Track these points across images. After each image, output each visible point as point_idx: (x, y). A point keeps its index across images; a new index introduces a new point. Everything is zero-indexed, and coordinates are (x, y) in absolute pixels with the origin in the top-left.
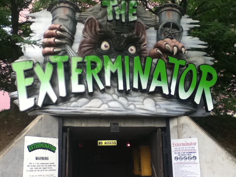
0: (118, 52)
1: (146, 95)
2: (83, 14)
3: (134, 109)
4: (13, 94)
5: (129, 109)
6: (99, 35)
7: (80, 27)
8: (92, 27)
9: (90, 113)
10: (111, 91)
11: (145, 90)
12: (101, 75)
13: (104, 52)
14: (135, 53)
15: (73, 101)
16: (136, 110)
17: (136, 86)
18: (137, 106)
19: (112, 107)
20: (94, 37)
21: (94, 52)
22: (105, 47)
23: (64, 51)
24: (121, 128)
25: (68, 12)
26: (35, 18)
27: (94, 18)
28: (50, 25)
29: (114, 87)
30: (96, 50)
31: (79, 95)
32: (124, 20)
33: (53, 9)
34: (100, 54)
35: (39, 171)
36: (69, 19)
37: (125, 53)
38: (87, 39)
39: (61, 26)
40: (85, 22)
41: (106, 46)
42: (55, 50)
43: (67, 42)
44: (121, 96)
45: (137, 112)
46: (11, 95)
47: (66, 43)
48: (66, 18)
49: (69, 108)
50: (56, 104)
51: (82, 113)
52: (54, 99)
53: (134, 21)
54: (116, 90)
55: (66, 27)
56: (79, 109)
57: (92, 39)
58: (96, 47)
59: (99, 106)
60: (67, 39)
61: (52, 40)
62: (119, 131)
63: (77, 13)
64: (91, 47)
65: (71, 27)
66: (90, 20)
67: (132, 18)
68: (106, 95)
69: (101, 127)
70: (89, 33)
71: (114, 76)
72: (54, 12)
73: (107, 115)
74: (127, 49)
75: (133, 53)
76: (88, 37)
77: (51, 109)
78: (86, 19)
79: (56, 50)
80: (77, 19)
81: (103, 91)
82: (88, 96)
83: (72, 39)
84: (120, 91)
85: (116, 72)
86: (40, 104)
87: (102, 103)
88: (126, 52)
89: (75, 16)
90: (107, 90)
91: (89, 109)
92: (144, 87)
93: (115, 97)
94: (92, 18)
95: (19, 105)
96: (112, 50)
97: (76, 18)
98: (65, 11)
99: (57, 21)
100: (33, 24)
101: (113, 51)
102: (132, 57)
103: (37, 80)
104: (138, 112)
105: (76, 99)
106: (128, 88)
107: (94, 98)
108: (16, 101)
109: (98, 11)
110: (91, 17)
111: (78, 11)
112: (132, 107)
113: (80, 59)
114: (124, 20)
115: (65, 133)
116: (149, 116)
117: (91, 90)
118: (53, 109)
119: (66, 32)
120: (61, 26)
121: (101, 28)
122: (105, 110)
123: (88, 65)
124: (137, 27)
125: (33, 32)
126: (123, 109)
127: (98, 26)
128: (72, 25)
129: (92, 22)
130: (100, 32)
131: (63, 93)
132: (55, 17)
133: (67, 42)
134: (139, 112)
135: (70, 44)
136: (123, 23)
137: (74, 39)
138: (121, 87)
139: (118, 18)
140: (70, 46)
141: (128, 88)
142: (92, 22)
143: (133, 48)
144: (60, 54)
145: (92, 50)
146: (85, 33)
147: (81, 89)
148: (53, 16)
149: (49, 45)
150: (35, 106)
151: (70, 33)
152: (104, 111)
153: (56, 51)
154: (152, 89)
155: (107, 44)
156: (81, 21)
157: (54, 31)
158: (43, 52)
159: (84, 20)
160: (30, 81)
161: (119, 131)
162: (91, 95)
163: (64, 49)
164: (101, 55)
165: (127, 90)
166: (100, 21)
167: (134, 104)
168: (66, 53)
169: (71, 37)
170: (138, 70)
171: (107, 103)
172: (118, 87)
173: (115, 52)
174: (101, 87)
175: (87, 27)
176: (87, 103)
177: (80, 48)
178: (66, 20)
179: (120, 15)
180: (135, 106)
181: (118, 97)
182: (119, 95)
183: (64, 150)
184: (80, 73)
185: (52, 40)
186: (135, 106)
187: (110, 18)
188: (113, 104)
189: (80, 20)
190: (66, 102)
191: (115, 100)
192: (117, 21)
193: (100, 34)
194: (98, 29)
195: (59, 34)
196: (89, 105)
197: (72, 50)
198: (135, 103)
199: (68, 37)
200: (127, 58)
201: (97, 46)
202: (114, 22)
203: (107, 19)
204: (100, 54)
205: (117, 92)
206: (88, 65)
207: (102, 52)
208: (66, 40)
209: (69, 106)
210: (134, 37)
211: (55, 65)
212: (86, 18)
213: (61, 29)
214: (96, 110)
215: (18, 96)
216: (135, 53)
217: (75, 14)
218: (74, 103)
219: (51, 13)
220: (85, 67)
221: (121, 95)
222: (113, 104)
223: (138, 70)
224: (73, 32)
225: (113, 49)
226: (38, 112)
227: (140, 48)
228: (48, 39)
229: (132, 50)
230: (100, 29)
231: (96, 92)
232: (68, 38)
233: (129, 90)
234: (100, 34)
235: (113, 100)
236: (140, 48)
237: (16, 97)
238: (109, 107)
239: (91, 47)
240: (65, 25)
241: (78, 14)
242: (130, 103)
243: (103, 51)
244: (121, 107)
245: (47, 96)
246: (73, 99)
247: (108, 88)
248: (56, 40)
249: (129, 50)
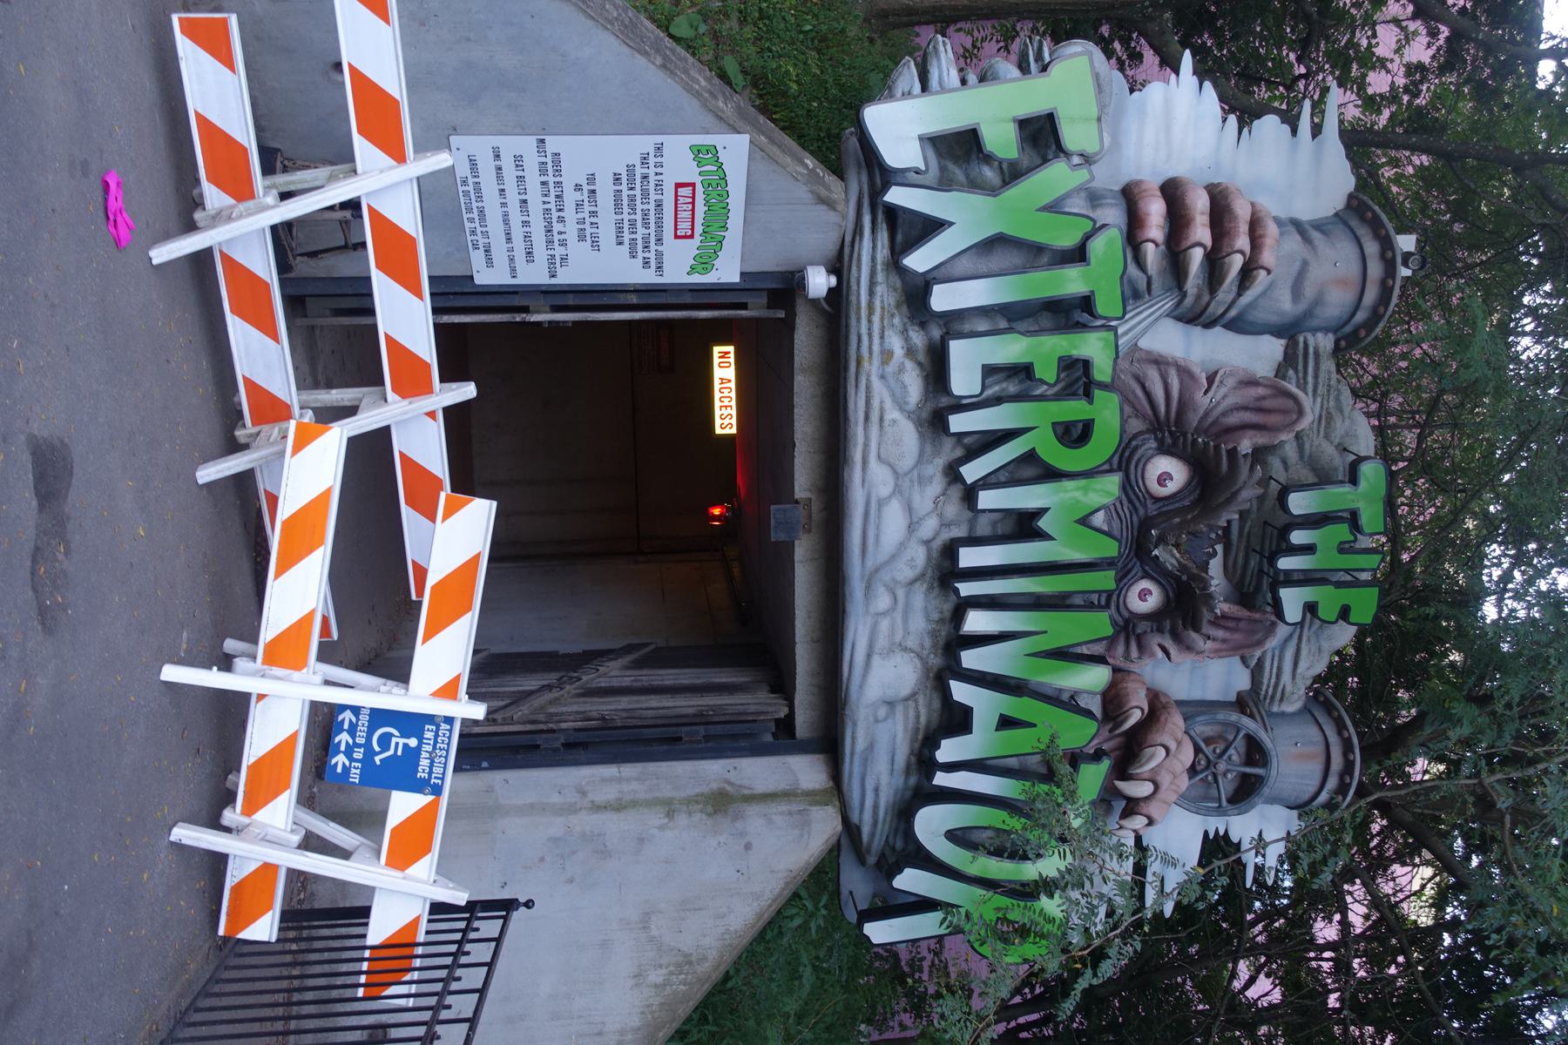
0: (1136, 533)
1: (936, 661)
2: (1328, 365)
3: (872, 610)
4: (943, 55)
5: (868, 588)
6: (1217, 447)
7: (1263, 354)
8: (1260, 410)
9: (847, 596)
10: (953, 508)
11: (958, 661)
12: (1033, 470)
13: (1136, 467)
14: (1130, 612)
15: (907, 339)
16: (869, 621)
17: (977, 622)
18: (884, 624)
19: (879, 517)
20: (1210, 420)
21: (1136, 425)
22: (1165, 473)
23: (1145, 286)
24: (789, 548)
25: (1337, 302)
26: (1314, 136)
27: (1305, 423)
28: (1273, 207)
29: (972, 523)
30: (1148, 431)
31: (936, 369)
32: (1285, 563)
33: (1354, 223)
34: (1127, 454)
35: (593, 214)
36: (1302, 307)
37: (1130, 566)
38: (1204, 390)
39: (1269, 272)
40: (1284, 378)
41: (1163, 479)
42: (1150, 247)
43: (1189, 301)
44: (929, 550)
45: (856, 624)
46: (941, 43)
47: (1184, 295)
48: (1309, 292)
49: (876, 319)
50: (895, 264)
51: (853, 383)
52: (919, 261)
53: (1279, 613)
54: (960, 532)
55: (1263, 294)
56: (872, 368)
57: (1202, 412)
58: (1163, 435)
59: (882, 455)
60: (1206, 298)
61: (1201, 232)
62: (773, 540)
63: (1331, 337)
64: (1162, 409)
65: (1261, 316)
66: (1290, 404)
67: (1292, 600)
68: (937, 485)
69: (794, 457)
70: (1230, 401)
71: (1024, 526)
72: (1339, 231)
73: (845, 535)
74: (1146, 576)
75: (1128, 600)
76: (1210, 394)
77: (874, 241)
78: (1298, 387)
79: (1151, 253)
80: (1301, 339)
81: (952, 473)
82: (930, 406)
83: (1203, 317)
84: (950, 551)
85: (1041, 535)
86: (896, 196)
87: (899, 471)
88: (1133, 573)
89: (1315, 330)
90: (956, 492)
91: (875, 417)
92: (971, 659)
93: (929, 527)
94: (1301, 412)
95: (891, 97)
96: (1145, 506)
97: (1309, 336)
98: (1342, 282)
99: (1293, 243)
100: (1286, 128)
101: (1141, 512)
102: (1108, 600)
103: (1012, 174)
104: (860, 627)
105: (921, 357)
106: (966, 589)
107: (921, 435)
108: (911, 73)
109: (1337, 436)
110: (1308, 409)
111: (1343, 343)
112: (883, 601)
113: (1102, 369)
114: (1285, 563)
115: (764, 301)
116: (842, 676)
117: (959, 423)
118: (872, 249)
119: (1239, 295)
120: (1269, 272)
121: (1250, 459)
122: (866, 485)
123: (1074, 410)
124: (1250, 620)
125: (1246, 130)
126: (870, 563)
127: (1261, 439)
128: (1273, 319)
129: (1284, 412)
130: (1233, 453)
131: (943, 299)
132: (1315, 235)
133: (1189, 301)
134: (858, 633)
135: (1180, 311)
136: (1272, 560)
137: (1209, 325)
138: (969, 557)
139: (1298, 537)
140: (1172, 311)
141: (966, 589)
142: (1284, 412)
143: (1153, 601)
144: (1133, 270)
145: (1150, 412)
146: (1230, 382)
147: (964, 379)
148: (1319, 226)
149: (1177, 219)
150: (880, 174)
151: (1233, 313)
152: (863, 481)
153: (1146, 251)
154: (961, 691)
155: (1172, 487)
156: (1290, 359)
157: (1243, 242)
158: (1144, 187)
159: (1296, 372)
160: (1001, 140)
161: (773, 540)
162: (935, 422)
163: (1155, 286)
164: (1125, 461)
165: (956, 585)
166: (1290, 451)
167: (893, 608)
168: (1133, 295)
169: (1213, 318)
170: (1046, 632)
171: (897, 489)
172: (974, 541)
173: (1135, 518)
174: (972, 471)
175: (1261, 391)
176: (901, 405)
177: (1159, 362)
178: (1297, 291)
179: (1309, 549)
180: (884, 614)
181: (927, 543)
182: (937, 544)
183: (688, 299)
184: (1039, 373)
185: (1201, 232)
186: (884, 614)
187: (1299, 503)
188: (893, 524)
189: (1295, 355)
190: (905, 309)
191: (912, 527)
192: (1285, 531)
193: (1224, 453)
194: (1251, 439)
195: (1230, 266)
196: (893, 414)
197: (1157, 320)
198: (898, 616)
199: (1213, 304)
200: (1104, 580)
201: (1169, 441)
202: (1282, 519)
203: (1255, 997)
204: (1127, 454)
205: (947, 535)
206: (1074, 410)
207: (1139, 460)
208: (1199, 297)
209: (886, 322)
210: (1205, 610)
211: (1078, 255)
212: (1305, 391)
213: (1255, 272)
214: (866, 445)
215: (937, 93)
216: (1131, 609)
217: (1326, 330)
218: (896, 344)
219: (1336, 215)
220: (1067, 393)
221: (935, 554)
222: (893, 524)
223: (1046, 632)
224: (1239, 325)
225: (1152, 509)
226: (857, 182)
227: (1152, 631)
228: (1203, 225)
229: (1143, 595)
230: (1245, 456)
231: (948, 443)
232: (1208, 304)
233: (957, 591)
234: (1224, 453)
235: (915, 520)
236: (1152, 631)
237: (931, 70)
238: (881, 503)
239: (1162, 409)
240: (1271, 286)
241: (1325, 342)
242: (901, 593)
243: (1140, 466)
244: (882, 558)
245: (930, 227)
246: (918, 338)
247: (970, 495)
248: (1197, 255)
249: (1145, 584)
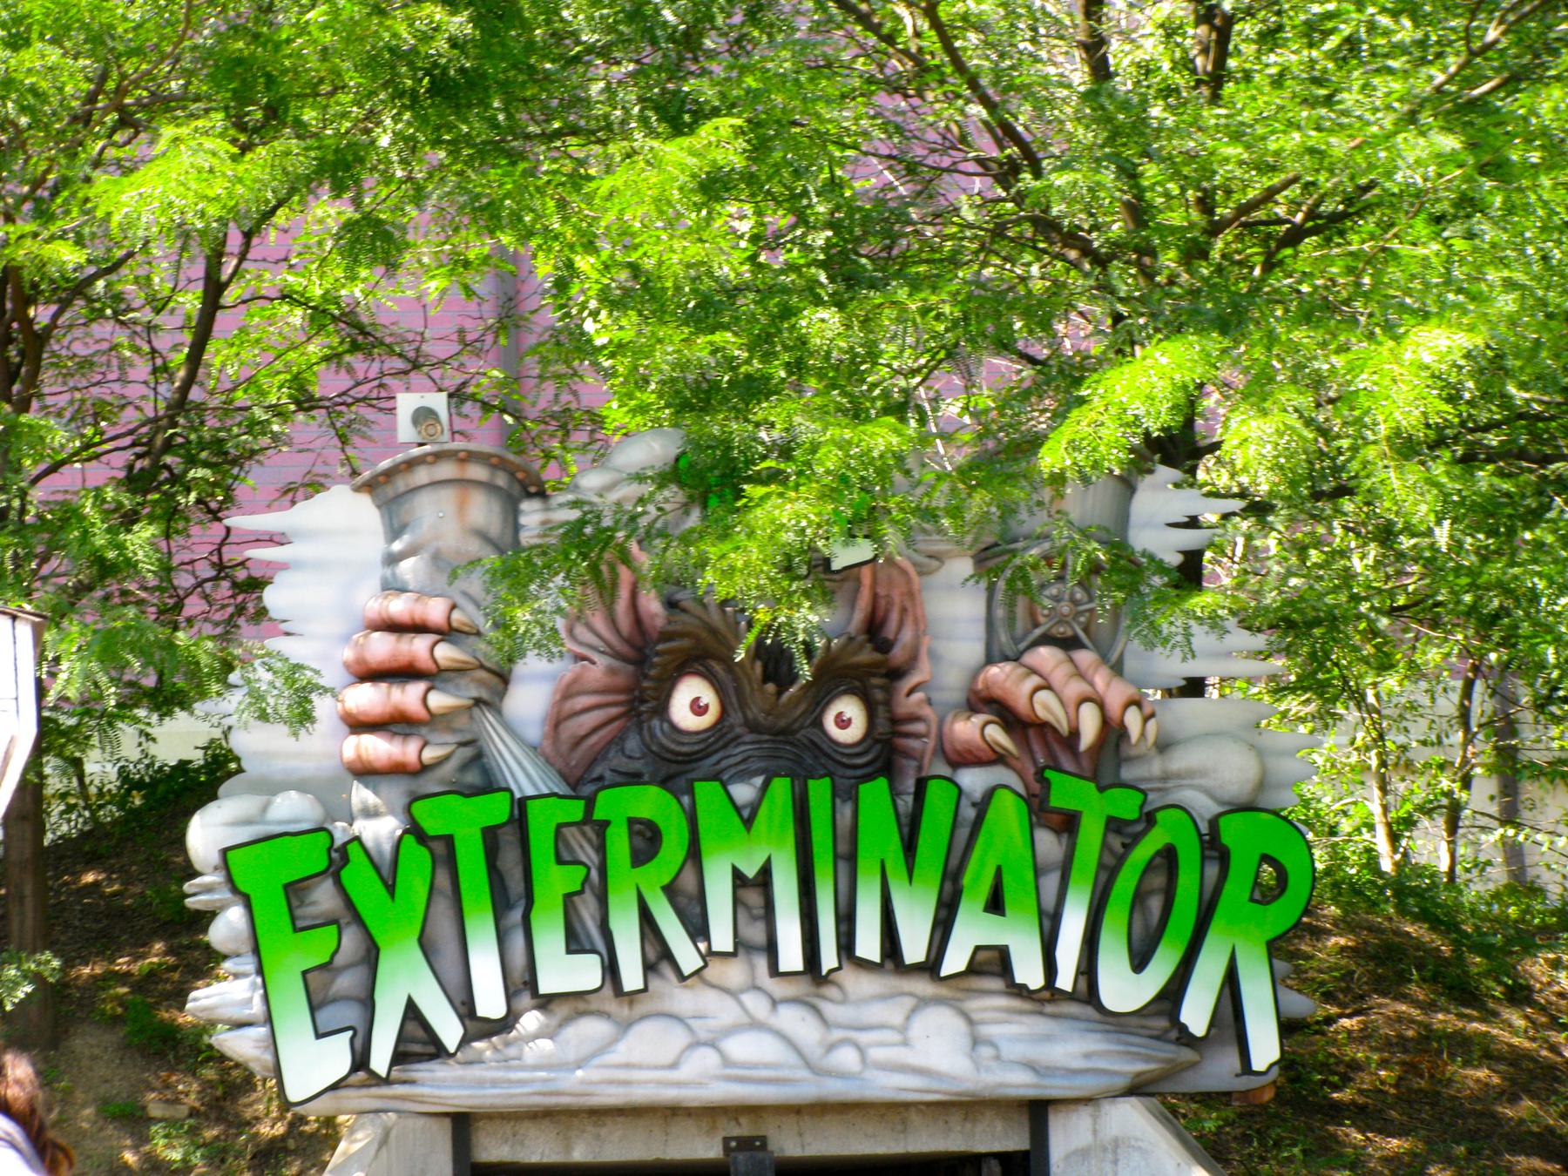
0: (766, 737)
17: (868, 944)
18: (877, 1054)
31: (574, 1003)
39: (454, 607)
41: (698, 708)
52: (449, 1030)
63: (526, 506)
85: (766, 872)
89: (517, 528)
91: (622, 1075)
92: (914, 948)
98: (461, 508)
101: (739, 730)
111: (533, 489)
112: (846, 1058)
123: (619, 844)
134: (886, 1086)
138: (791, 955)
154: (955, 960)
155: (708, 696)
171: (712, 1044)
172: (771, 949)
174: (687, 955)
180: (861, 1050)
191: (755, 1025)
198: (864, 1038)
206: (619, 844)
214: (659, 1083)
222: (746, 1048)
229: (843, 723)
238: (727, 1062)
239: (614, 711)
242: (837, 1034)
243: (686, 739)
